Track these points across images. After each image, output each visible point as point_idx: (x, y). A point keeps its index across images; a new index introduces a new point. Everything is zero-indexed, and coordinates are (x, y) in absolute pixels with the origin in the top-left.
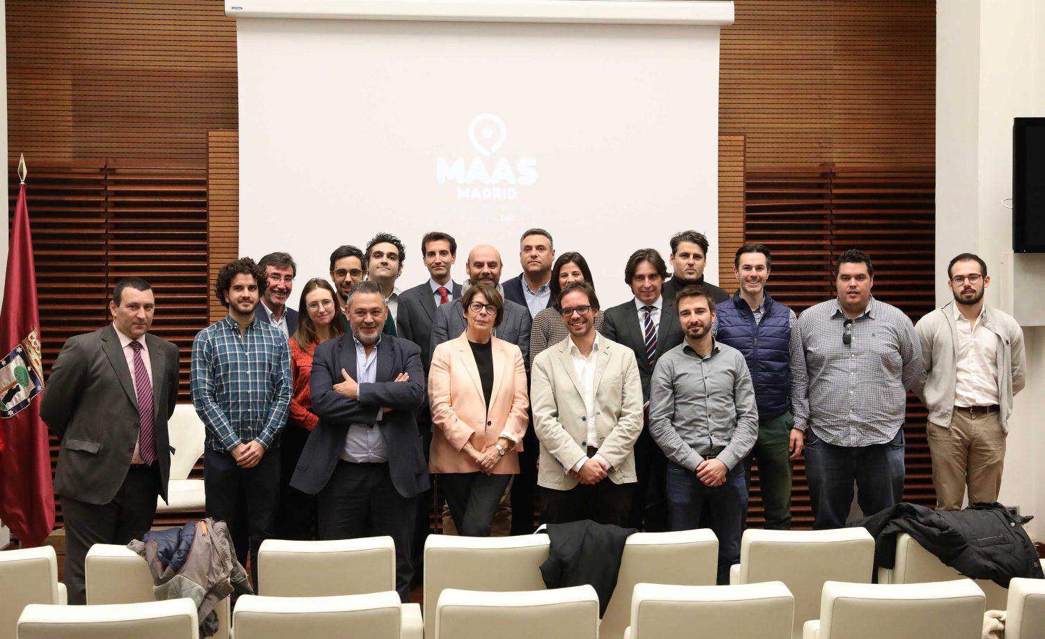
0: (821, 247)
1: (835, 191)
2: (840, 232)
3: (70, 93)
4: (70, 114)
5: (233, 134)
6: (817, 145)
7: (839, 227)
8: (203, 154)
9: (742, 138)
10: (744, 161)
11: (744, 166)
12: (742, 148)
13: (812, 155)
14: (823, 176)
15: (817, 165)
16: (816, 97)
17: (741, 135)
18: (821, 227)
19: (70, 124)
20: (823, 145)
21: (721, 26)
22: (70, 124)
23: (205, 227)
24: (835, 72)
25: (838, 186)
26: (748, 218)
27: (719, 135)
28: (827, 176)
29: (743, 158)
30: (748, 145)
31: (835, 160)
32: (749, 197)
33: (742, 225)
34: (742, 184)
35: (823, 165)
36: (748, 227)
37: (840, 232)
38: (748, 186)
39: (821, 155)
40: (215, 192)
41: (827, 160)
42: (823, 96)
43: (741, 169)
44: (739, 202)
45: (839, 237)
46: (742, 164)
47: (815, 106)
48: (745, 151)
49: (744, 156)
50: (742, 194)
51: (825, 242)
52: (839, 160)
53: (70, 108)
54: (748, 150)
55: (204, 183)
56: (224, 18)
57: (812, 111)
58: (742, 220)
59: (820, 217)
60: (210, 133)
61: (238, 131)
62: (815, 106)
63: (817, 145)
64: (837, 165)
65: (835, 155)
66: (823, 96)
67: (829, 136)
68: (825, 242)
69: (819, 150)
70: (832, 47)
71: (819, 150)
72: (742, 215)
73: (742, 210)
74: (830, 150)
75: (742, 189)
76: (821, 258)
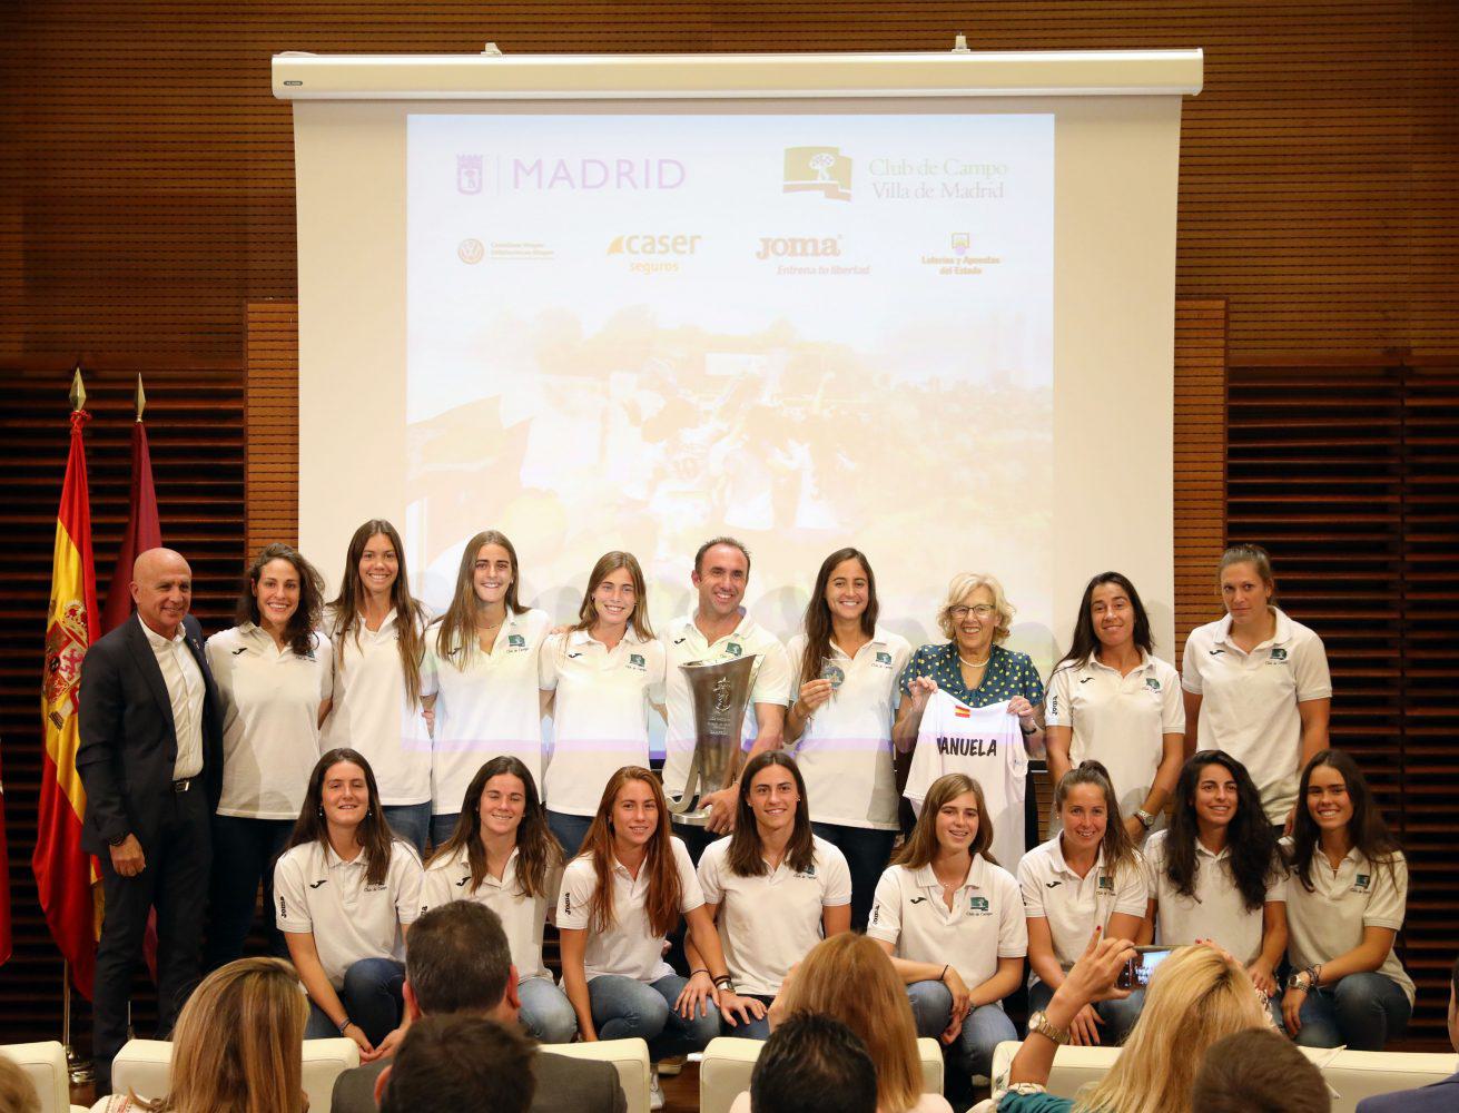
0: (1383, 509)
1: (1409, 403)
2: (1419, 480)
3: (19, 237)
4: (20, 274)
5: (289, 307)
6: (1378, 316)
7: (1419, 470)
8: (232, 340)
9: (1221, 304)
10: (1226, 348)
11: (1226, 357)
12: (1221, 324)
13: (1370, 334)
14: (1389, 373)
15: (1378, 352)
16: (1377, 223)
17: (1219, 299)
18: (1382, 471)
19: (20, 292)
20: (1391, 315)
21: (1184, 96)
22: (20, 292)
23: (239, 472)
24: (1416, 177)
25: (1417, 393)
26: (1232, 453)
27: (1177, 299)
28: (1394, 376)
29: (1222, 342)
30: (1233, 317)
31: (1414, 343)
32: (1233, 414)
33: (1220, 467)
34: (1221, 390)
35: (1391, 352)
36: (1232, 471)
37: (1419, 480)
38: (1232, 393)
39: (1385, 334)
40: (258, 411)
41: (1399, 344)
42: (1392, 223)
43: (1220, 362)
44: (1215, 423)
45: (1417, 490)
46: (1221, 352)
47: (1376, 242)
48: (1226, 329)
49: (1226, 338)
50: (1221, 410)
51: (1387, 499)
52: (1422, 343)
53: (21, 264)
54: (1232, 326)
55: (239, 395)
56: (269, 100)
57: (1368, 251)
58: (1220, 457)
59: (1382, 451)
60: (251, 306)
61: (297, 302)
62: (1376, 242)
63: (1378, 316)
64: (1415, 353)
65: (1413, 333)
66: (1392, 223)
67: (1401, 297)
68: (1387, 499)
69: (1385, 325)
70: (1409, 130)
71: (1385, 325)
72: (1221, 447)
73: (1220, 438)
74: (1405, 325)
75: (1221, 400)
76: (1381, 528)
